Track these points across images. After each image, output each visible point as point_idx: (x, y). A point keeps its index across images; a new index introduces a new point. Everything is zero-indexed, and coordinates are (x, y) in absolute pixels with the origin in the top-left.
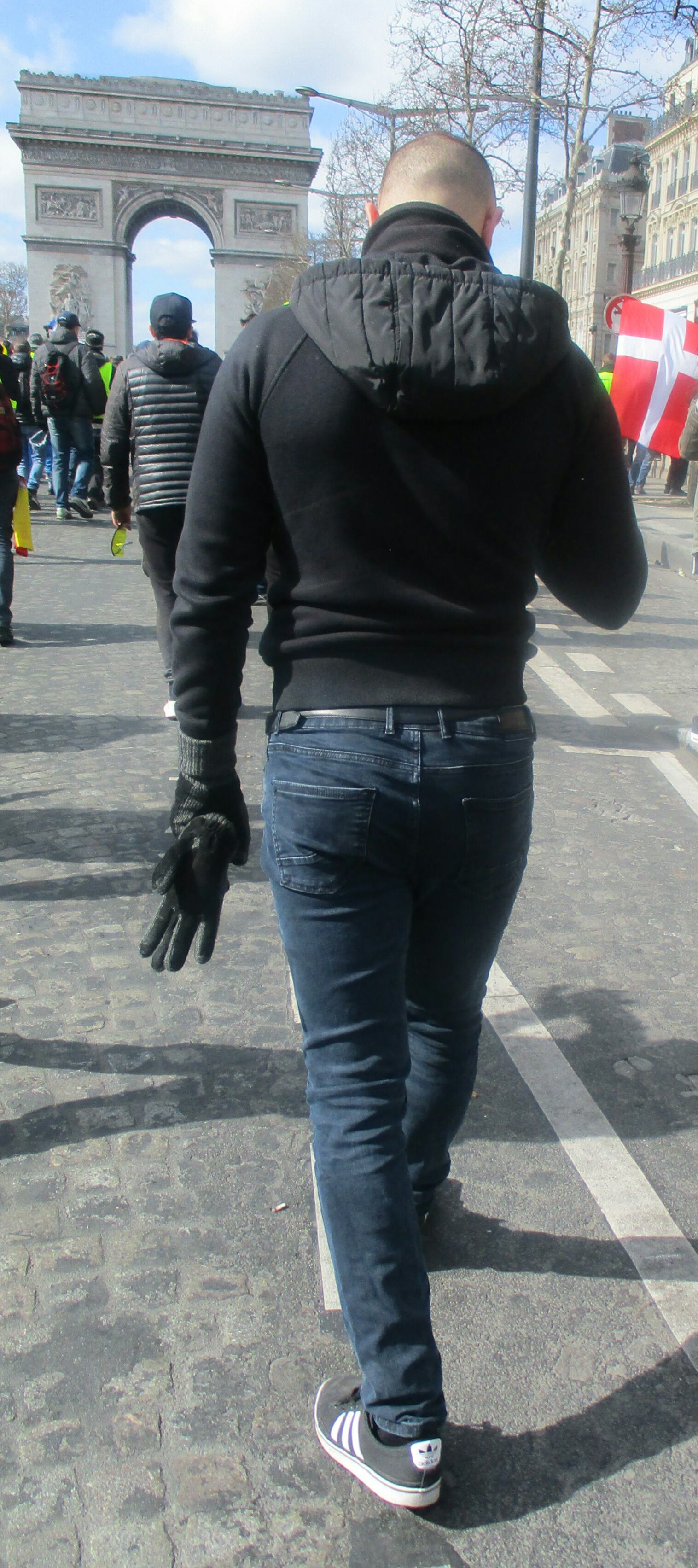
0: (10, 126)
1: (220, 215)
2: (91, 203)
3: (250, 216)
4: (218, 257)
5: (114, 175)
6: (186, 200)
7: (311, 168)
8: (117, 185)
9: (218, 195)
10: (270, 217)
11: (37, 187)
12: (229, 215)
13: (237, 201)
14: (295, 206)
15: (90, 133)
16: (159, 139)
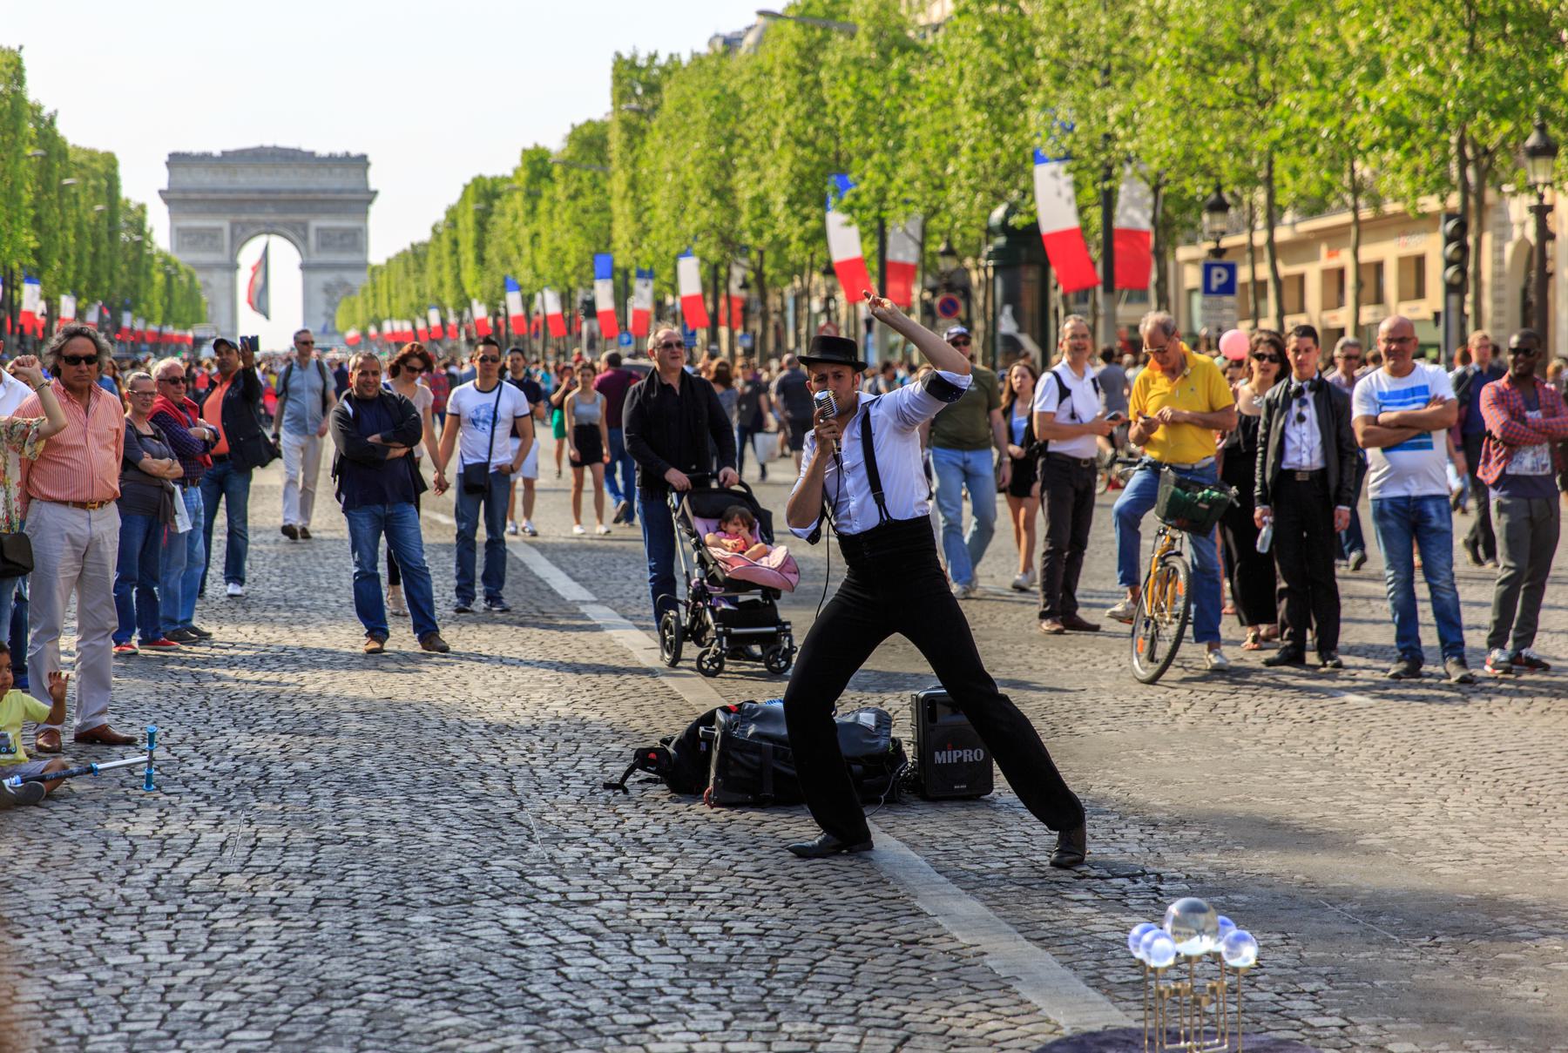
0: (161, 192)
1: (305, 239)
2: (215, 237)
3: (328, 240)
4: (304, 267)
5: (231, 217)
6: (282, 230)
7: (370, 202)
8: (233, 225)
9: (305, 227)
10: (342, 237)
11: (178, 229)
12: (312, 238)
13: (318, 230)
14: (360, 230)
15: (215, 191)
16: (262, 191)
